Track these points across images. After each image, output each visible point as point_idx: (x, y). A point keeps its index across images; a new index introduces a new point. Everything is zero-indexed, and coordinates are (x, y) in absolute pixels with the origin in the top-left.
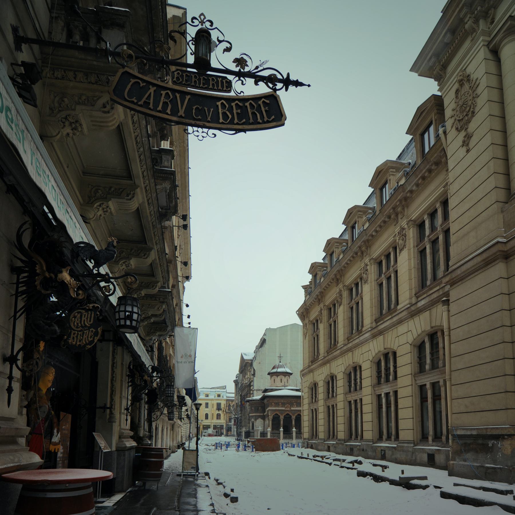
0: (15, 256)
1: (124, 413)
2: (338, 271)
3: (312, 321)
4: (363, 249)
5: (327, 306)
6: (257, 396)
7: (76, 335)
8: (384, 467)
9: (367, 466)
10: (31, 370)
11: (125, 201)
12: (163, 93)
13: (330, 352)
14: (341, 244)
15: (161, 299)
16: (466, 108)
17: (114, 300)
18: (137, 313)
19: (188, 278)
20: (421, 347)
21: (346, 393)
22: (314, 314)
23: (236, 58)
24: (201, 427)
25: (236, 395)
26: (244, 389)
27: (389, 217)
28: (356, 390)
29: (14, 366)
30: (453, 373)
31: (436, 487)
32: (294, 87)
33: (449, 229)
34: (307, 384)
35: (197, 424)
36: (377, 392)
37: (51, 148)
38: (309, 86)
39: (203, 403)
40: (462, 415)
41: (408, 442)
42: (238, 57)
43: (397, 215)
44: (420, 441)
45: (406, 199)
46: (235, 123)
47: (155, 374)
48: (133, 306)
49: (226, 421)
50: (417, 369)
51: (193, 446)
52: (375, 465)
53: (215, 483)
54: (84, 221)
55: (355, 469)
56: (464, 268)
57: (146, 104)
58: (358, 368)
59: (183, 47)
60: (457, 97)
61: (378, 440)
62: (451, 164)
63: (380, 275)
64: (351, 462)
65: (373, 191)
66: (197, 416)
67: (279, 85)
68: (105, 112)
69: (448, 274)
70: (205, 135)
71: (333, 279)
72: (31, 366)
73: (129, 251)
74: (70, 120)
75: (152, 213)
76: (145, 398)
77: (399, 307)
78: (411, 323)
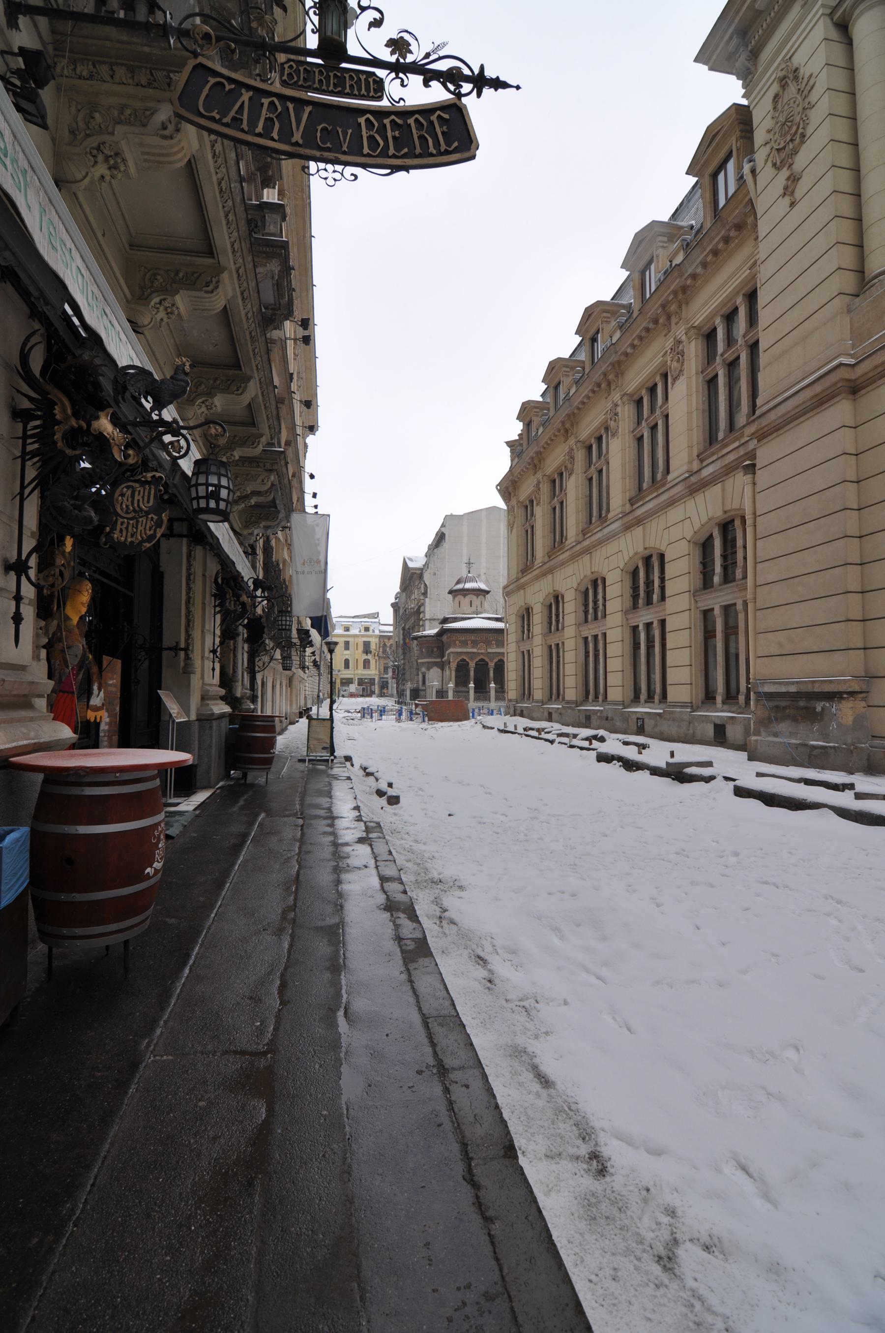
0: (19, 391)
1: (208, 658)
2: (568, 415)
3: (522, 502)
4: (611, 377)
5: (549, 476)
7: (125, 525)
8: (642, 747)
9: (613, 745)
10: (53, 585)
11: (202, 294)
12: (266, 101)
13: (554, 554)
14: (572, 368)
15: (268, 466)
16: (790, 128)
17: (186, 466)
18: (228, 488)
19: (312, 429)
20: (706, 546)
21: (580, 624)
22: (526, 490)
23: (391, 39)
24: (338, 682)
25: (395, 628)
26: (409, 618)
27: (656, 322)
29: (23, 578)
30: (758, 589)
31: (727, 779)
32: (492, 90)
33: (757, 342)
34: (514, 609)
35: (331, 678)
36: (630, 621)
37: (73, 201)
38: (518, 88)
39: (341, 641)
40: (773, 660)
41: (683, 705)
42: (395, 37)
43: (669, 318)
44: (703, 703)
45: (684, 289)
46: (390, 154)
47: (259, 593)
48: (219, 475)
49: (379, 671)
50: (699, 583)
51: (324, 712)
52: (626, 743)
53: (362, 773)
54: (134, 330)
55: (594, 750)
56: (781, 410)
57: (236, 122)
58: (599, 582)
59: (300, 21)
60: (774, 108)
61: (632, 701)
62: (763, 228)
63: (639, 423)
64: (587, 739)
65: (629, 276)
66: (331, 663)
67: (466, 87)
68: (165, 137)
69: (753, 421)
70: (338, 176)
71: (559, 431)
72: (51, 579)
73: (211, 382)
74: (105, 151)
75: (249, 315)
76: (243, 632)
77: (670, 477)
78: (690, 504)
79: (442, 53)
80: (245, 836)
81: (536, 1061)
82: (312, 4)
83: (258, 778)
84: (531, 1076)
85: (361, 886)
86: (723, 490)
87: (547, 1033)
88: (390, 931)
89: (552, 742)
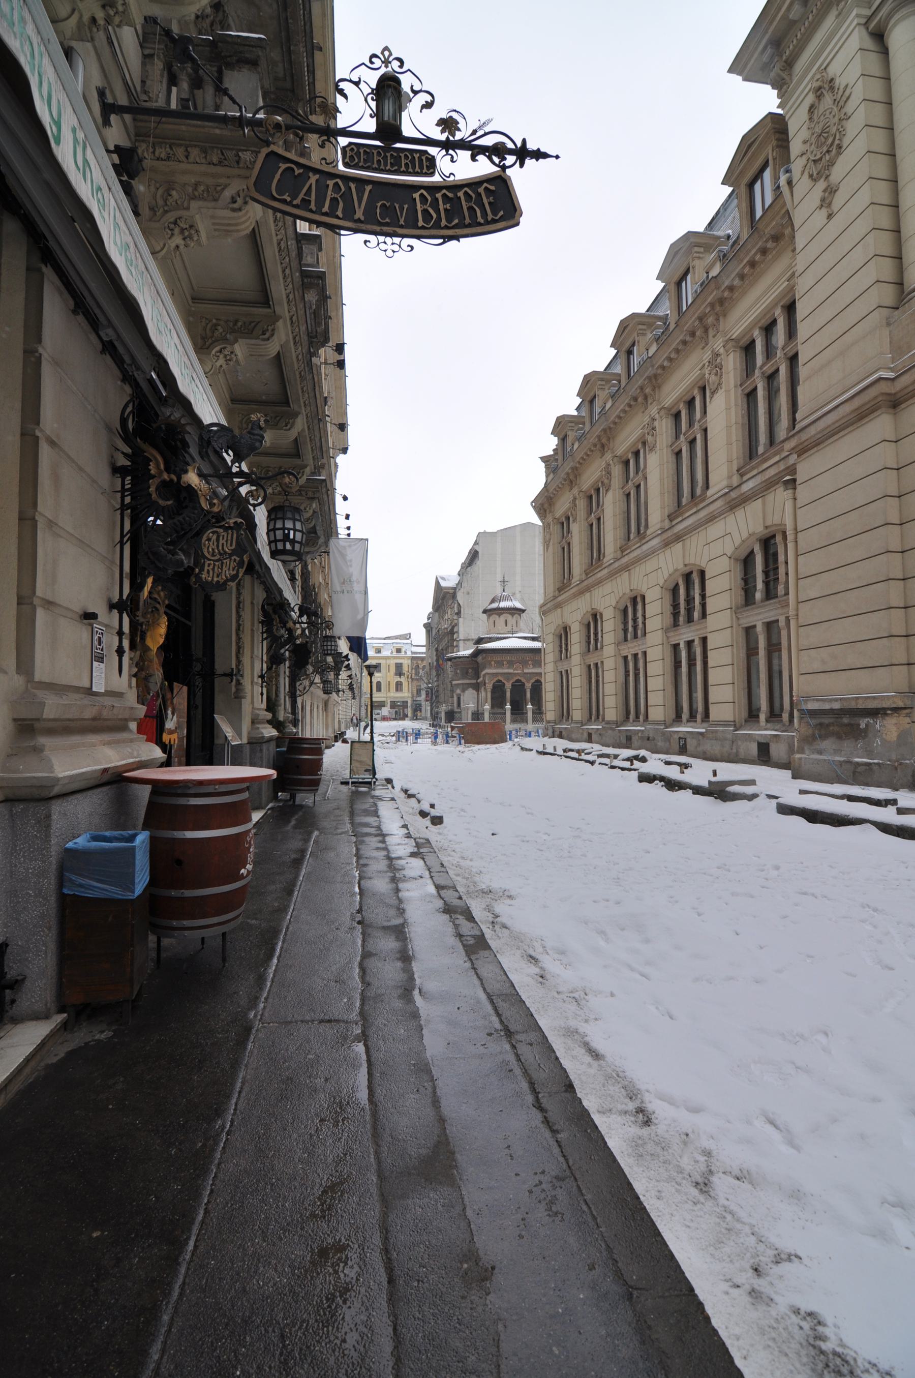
2: (604, 430)
3: (558, 519)
5: (585, 492)
6: (466, 651)
8: (685, 766)
9: (655, 765)
13: (592, 571)
20: (747, 562)
21: (619, 643)
22: (562, 507)
28: (636, 636)
30: (801, 605)
31: (770, 797)
34: (552, 629)
36: (671, 639)
40: (817, 675)
41: (726, 724)
44: (746, 721)
52: (668, 763)
55: (635, 770)
58: (639, 599)
61: (674, 721)
64: (628, 759)
65: (664, 287)
71: (595, 445)
77: (709, 493)
78: (731, 519)
79: (487, 129)
80: (303, 852)
81: (587, 1039)
82: (370, 91)
83: (305, 798)
84: (583, 1051)
85: (419, 893)
86: (764, 504)
87: (596, 1019)
88: (450, 929)
89: (592, 763)
